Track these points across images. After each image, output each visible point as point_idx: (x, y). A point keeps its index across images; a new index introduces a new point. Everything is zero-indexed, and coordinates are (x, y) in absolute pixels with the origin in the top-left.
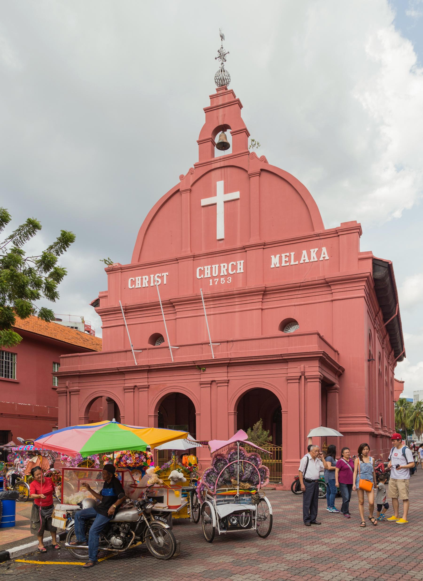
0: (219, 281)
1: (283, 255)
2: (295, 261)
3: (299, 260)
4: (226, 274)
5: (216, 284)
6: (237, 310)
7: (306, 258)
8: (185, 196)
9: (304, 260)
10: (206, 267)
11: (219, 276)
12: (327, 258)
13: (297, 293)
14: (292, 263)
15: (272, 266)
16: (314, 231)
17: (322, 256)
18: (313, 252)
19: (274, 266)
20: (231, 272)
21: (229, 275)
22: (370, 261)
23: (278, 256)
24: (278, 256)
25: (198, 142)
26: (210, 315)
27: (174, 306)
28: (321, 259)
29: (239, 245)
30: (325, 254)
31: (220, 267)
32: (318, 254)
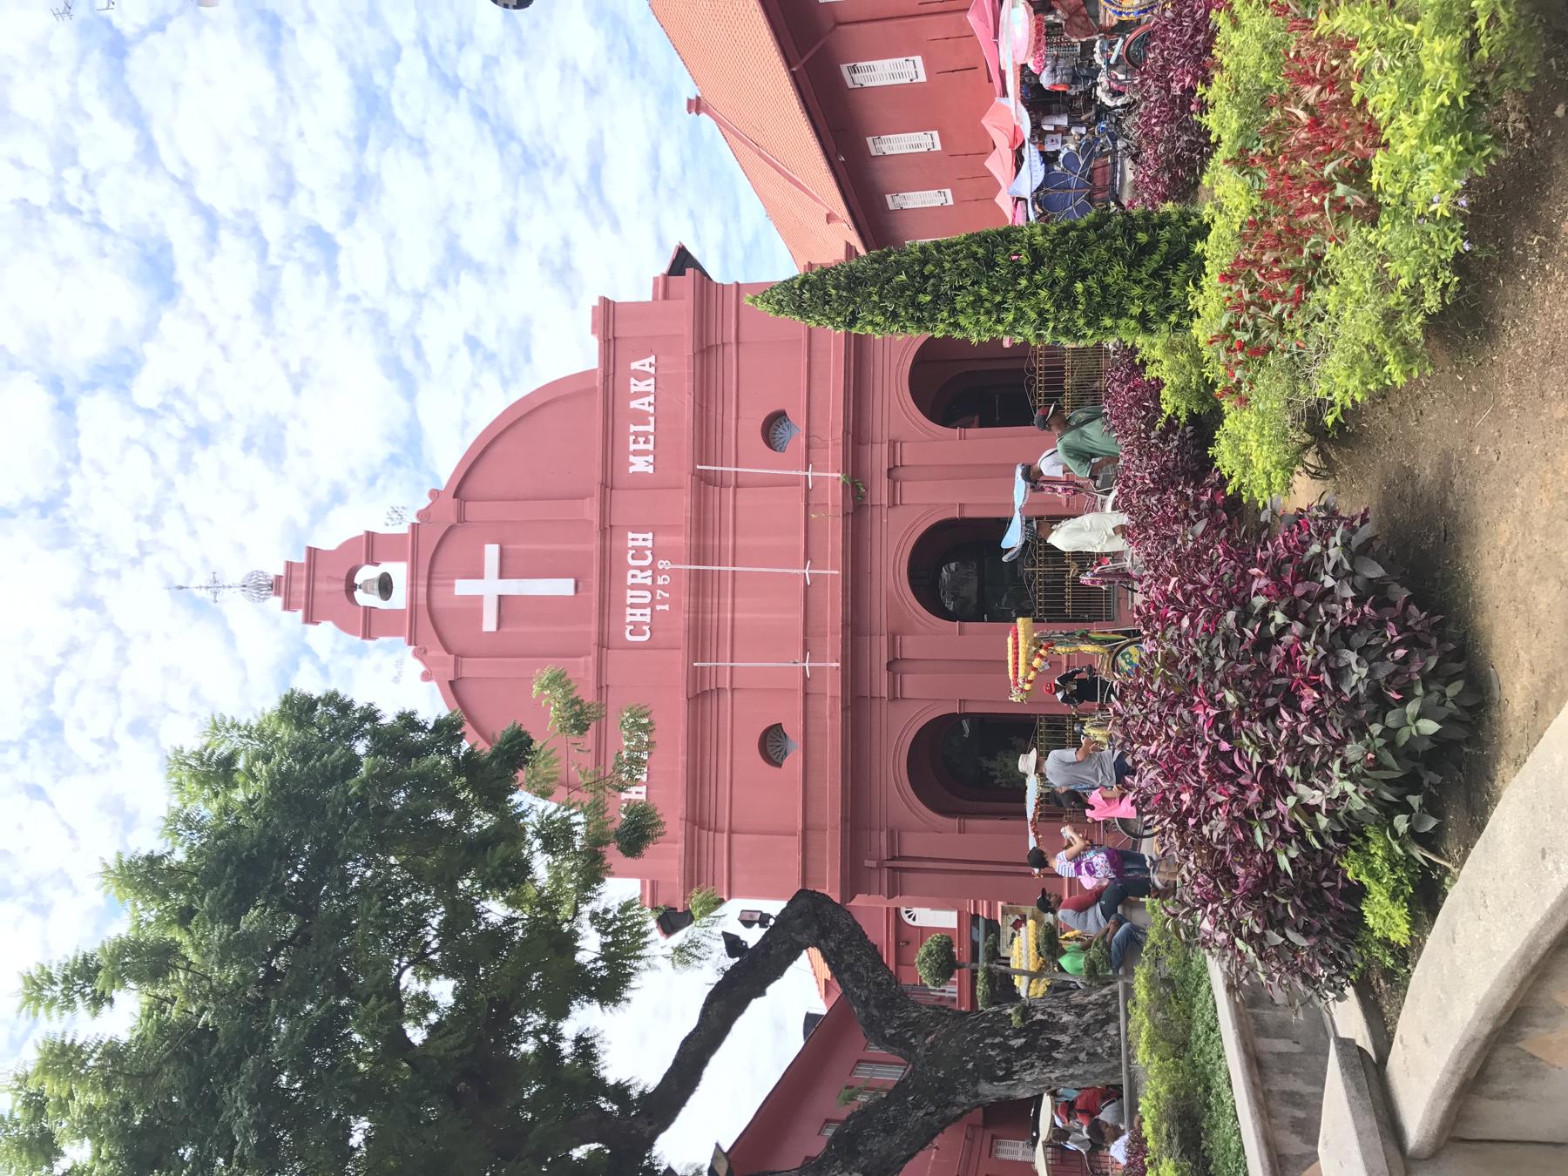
0: (664, 588)
1: (632, 447)
2: (648, 423)
3: (647, 414)
4: (649, 573)
5: (667, 595)
6: (731, 543)
7: (646, 400)
8: (470, 668)
9: (650, 404)
10: (629, 619)
11: (652, 589)
12: (652, 359)
13: (713, 414)
14: (651, 428)
15: (650, 469)
16: (595, 389)
17: (647, 368)
18: (636, 386)
19: (651, 467)
20: (646, 563)
21: (653, 566)
22: (672, 278)
23: (632, 459)
24: (632, 459)
25: (364, 637)
26: (733, 603)
27: (704, 693)
28: (652, 370)
29: (594, 545)
30: (644, 364)
31: (634, 587)
32: (641, 376)
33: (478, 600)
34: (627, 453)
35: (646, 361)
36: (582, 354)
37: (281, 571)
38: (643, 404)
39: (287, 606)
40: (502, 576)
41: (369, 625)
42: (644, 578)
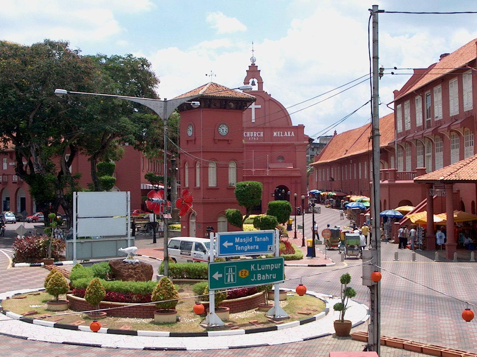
0: (253, 139)
1: (278, 132)
7: (287, 134)
11: (253, 137)
14: (282, 136)
15: (274, 136)
20: (258, 135)
23: (276, 132)
24: (276, 132)
30: (293, 134)
31: (253, 133)
36: (295, 123)
37: (255, 65)
38: (286, 134)
40: (255, 108)
41: (246, 82)
42: (255, 135)
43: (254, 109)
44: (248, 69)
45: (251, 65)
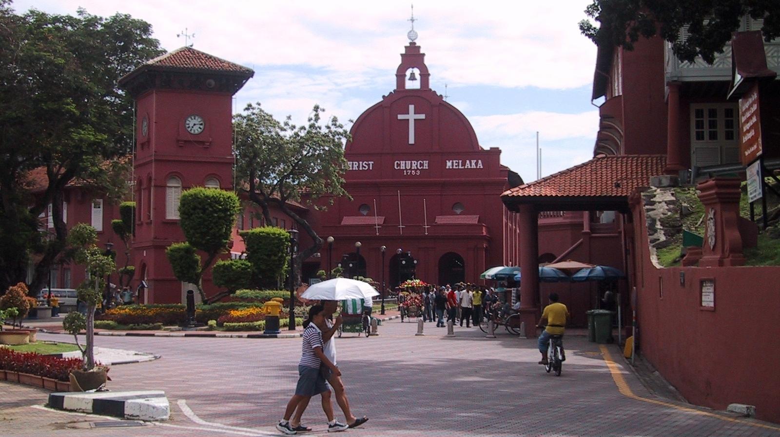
0: (411, 173)
3: (465, 166)
4: (416, 168)
11: (411, 169)
12: (482, 167)
14: (460, 167)
15: (447, 167)
17: (479, 165)
21: (418, 169)
22: (507, 173)
23: (451, 161)
24: (451, 161)
28: (478, 167)
30: (480, 165)
31: (411, 163)
32: (476, 164)
33: (407, 112)
34: (453, 160)
35: (481, 165)
37: (418, 44)
38: (468, 165)
39: (406, 47)
40: (415, 120)
41: (400, 76)
42: (414, 167)
43: (413, 120)
44: (403, 52)
45: (408, 45)
